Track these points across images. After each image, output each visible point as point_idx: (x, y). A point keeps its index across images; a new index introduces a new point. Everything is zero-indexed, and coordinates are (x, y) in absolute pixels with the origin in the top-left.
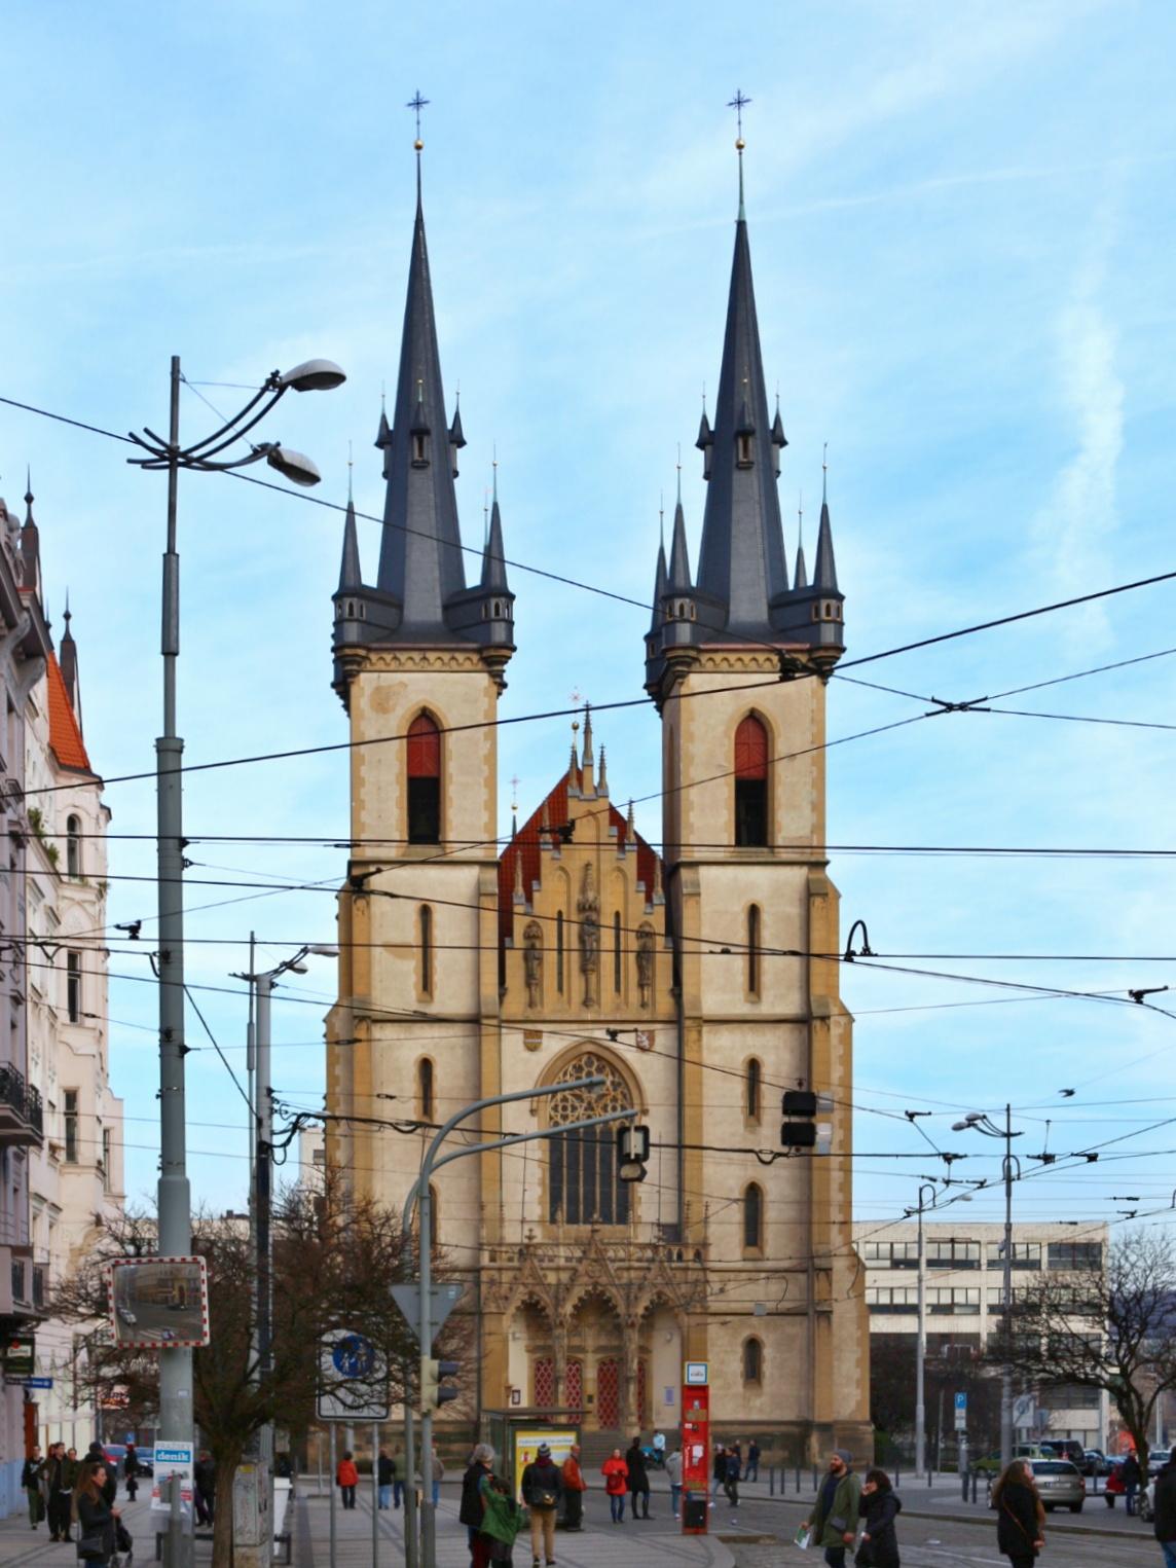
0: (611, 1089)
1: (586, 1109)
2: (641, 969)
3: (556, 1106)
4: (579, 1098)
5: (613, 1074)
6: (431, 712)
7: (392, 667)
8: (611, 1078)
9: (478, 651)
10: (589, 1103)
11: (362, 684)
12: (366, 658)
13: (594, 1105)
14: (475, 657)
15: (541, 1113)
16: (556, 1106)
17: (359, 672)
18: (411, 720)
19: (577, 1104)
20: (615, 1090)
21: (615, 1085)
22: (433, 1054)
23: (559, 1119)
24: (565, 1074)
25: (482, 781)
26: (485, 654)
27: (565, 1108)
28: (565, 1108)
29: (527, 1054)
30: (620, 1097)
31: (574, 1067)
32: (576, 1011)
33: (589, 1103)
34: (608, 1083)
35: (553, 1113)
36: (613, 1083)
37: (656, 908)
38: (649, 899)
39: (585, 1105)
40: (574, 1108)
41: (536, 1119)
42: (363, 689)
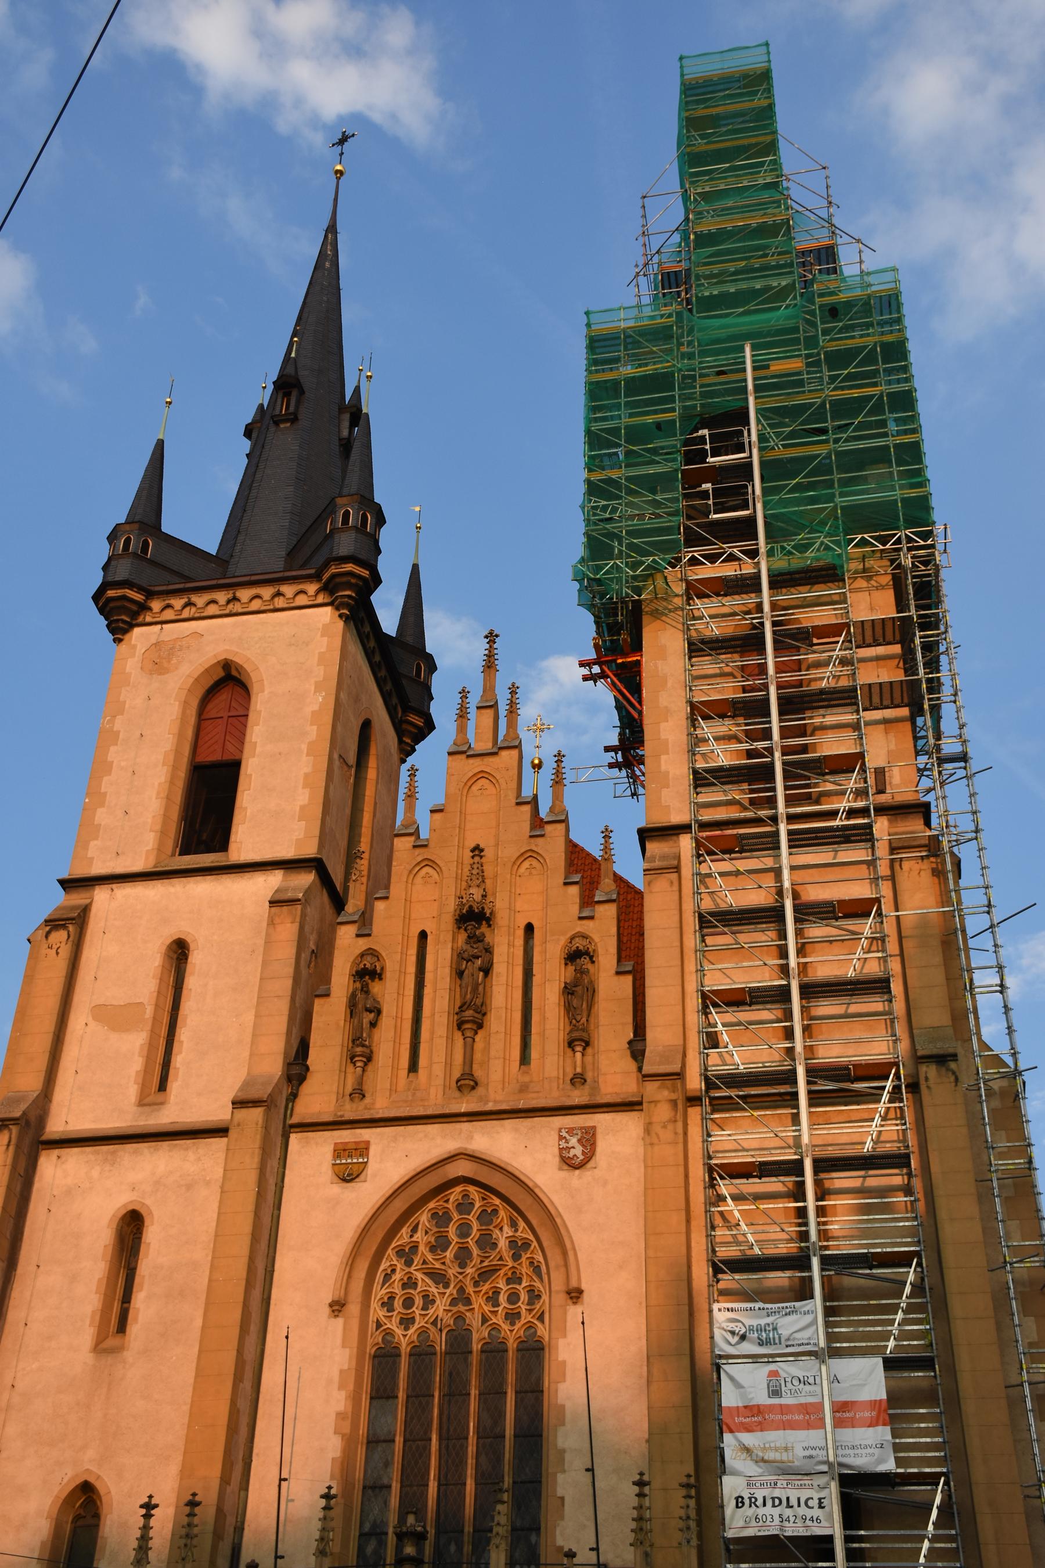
0: (507, 1255)
1: (454, 1302)
2: (570, 1010)
3: (392, 1298)
4: (439, 1278)
5: (514, 1225)
6: (239, 668)
7: (186, 613)
8: (508, 1231)
9: (316, 577)
10: (461, 1290)
11: (133, 642)
12: (144, 608)
13: (470, 1289)
14: (312, 588)
15: (354, 1308)
16: (392, 1298)
17: (131, 626)
18: (211, 683)
19: (433, 1290)
20: (516, 1257)
21: (518, 1247)
22: (148, 1202)
23: (393, 1325)
24: (415, 1230)
25: (304, 747)
26: (326, 577)
27: (408, 1303)
28: (408, 1303)
29: (337, 1189)
30: (525, 1269)
31: (434, 1215)
32: (435, 1101)
33: (461, 1290)
34: (503, 1243)
35: (382, 1313)
36: (512, 1243)
37: (600, 909)
38: (587, 901)
39: (452, 1290)
40: (428, 1301)
41: (340, 1321)
42: (134, 647)
